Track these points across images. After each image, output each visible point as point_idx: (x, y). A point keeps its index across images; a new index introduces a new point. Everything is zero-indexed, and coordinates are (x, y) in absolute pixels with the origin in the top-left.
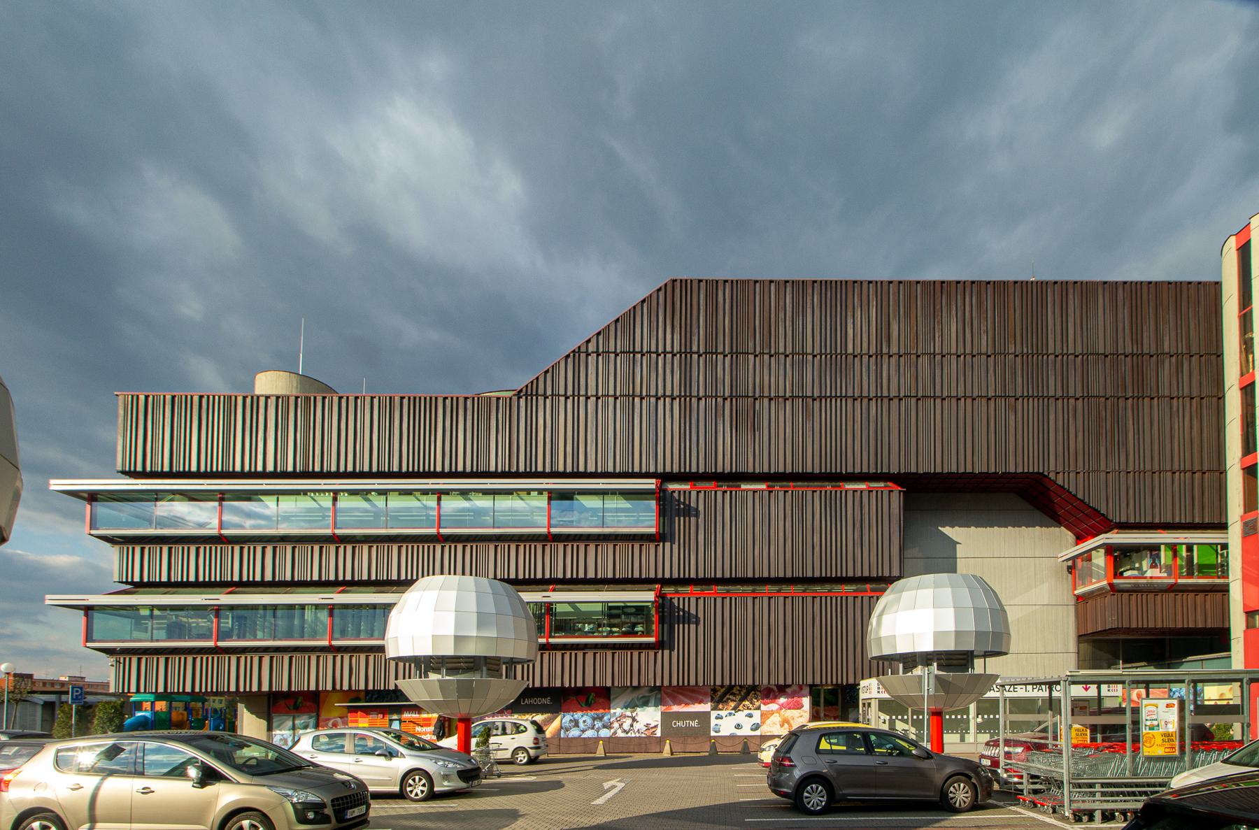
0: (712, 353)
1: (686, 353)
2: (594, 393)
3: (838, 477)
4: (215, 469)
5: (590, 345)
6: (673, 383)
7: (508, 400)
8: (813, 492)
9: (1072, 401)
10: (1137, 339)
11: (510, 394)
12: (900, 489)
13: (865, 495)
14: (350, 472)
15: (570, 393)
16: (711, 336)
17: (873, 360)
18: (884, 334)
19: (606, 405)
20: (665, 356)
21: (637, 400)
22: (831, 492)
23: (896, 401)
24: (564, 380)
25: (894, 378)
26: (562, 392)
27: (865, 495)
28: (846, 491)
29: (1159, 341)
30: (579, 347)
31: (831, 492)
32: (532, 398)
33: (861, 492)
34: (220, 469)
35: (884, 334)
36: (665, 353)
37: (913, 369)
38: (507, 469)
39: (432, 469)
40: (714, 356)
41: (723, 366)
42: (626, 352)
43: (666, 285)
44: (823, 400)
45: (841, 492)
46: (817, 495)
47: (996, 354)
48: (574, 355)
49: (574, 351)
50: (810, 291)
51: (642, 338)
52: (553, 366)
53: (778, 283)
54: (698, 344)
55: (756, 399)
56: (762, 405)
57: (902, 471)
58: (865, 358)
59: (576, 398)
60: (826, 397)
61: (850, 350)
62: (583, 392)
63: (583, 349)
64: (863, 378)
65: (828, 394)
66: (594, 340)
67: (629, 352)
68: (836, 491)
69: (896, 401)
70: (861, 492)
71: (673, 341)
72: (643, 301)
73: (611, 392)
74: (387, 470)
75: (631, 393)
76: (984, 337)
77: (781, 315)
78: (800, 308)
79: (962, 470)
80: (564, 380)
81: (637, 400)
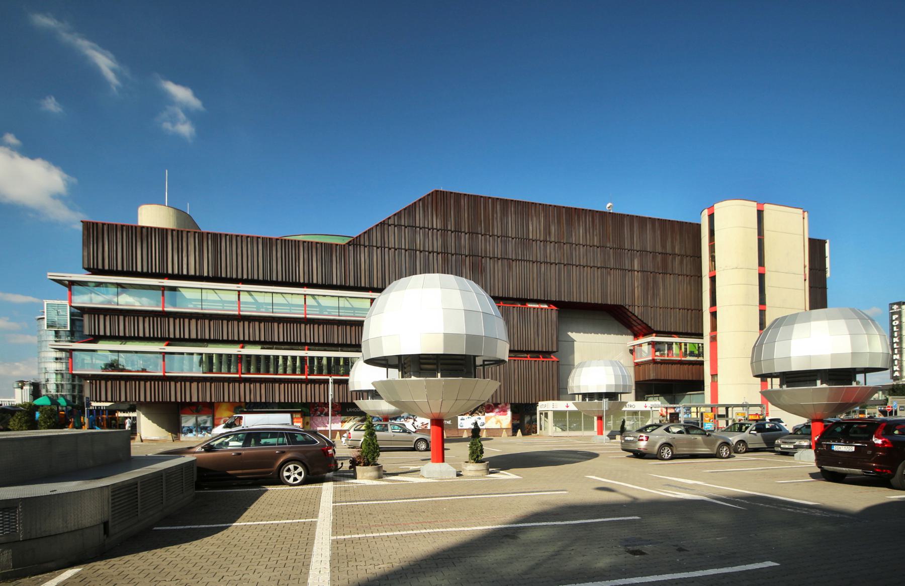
0: (459, 232)
1: (445, 230)
2: (393, 246)
3: (524, 301)
4: (154, 271)
5: (390, 220)
6: (438, 245)
7: (343, 247)
8: (514, 307)
9: (636, 272)
10: (664, 246)
11: (342, 241)
12: (556, 308)
13: (539, 310)
14: (245, 279)
15: (379, 245)
16: (458, 223)
17: (542, 243)
18: (548, 231)
19: (400, 254)
20: (433, 230)
21: (418, 252)
22: (520, 308)
23: (554, 265)
24: (376, 238)
25: (552, 253)
26: (375, 244)
27: (539, 310)
28: (527, 308)
29: (673, 248)
30: (384, 221)
31: (520, 308)
32: (357, 247)
33: (538, 309)
34: (157, 271)
35: (548, 231)
36: (433, 229)
37: (562, 250)
38: (343, 284)
39: (298, 281)
40: (460, 233)
41: (465, 239)
42: (411, 226)
43: (432, 193)
44: (518, 261)
45: (527, 308)
46: (515, 309)
47: (602, 247)
48: (381, 225)
49: (381, 223)
50: (510, 204)
51: (419, 220)
52: (369, 230)
53: (493, 199)
54: (451, 226)
55: (483, 258)
56: (486, 261)
57: (557, 300)
58: (538, 242)
59: (383, 249)
60: (519, 260)
61: (531, 237)
62: (386, 246)
63: (386, 222)
64: (537, 252)
65: (520, 259)
66: (392, 218)
67: (413, 227)
68: (522, 308)
69: (554, 265)
70: (538, 309)
71: (437, 223)
72: (420, 200)
73: (403, 247)
74: (269, 279)
75: (414, 248)
76: (595, 238)
77: (495, 215)
78: (504, 212)
79: (586, 301)
80: (376, 238)
81: (418, 252)
